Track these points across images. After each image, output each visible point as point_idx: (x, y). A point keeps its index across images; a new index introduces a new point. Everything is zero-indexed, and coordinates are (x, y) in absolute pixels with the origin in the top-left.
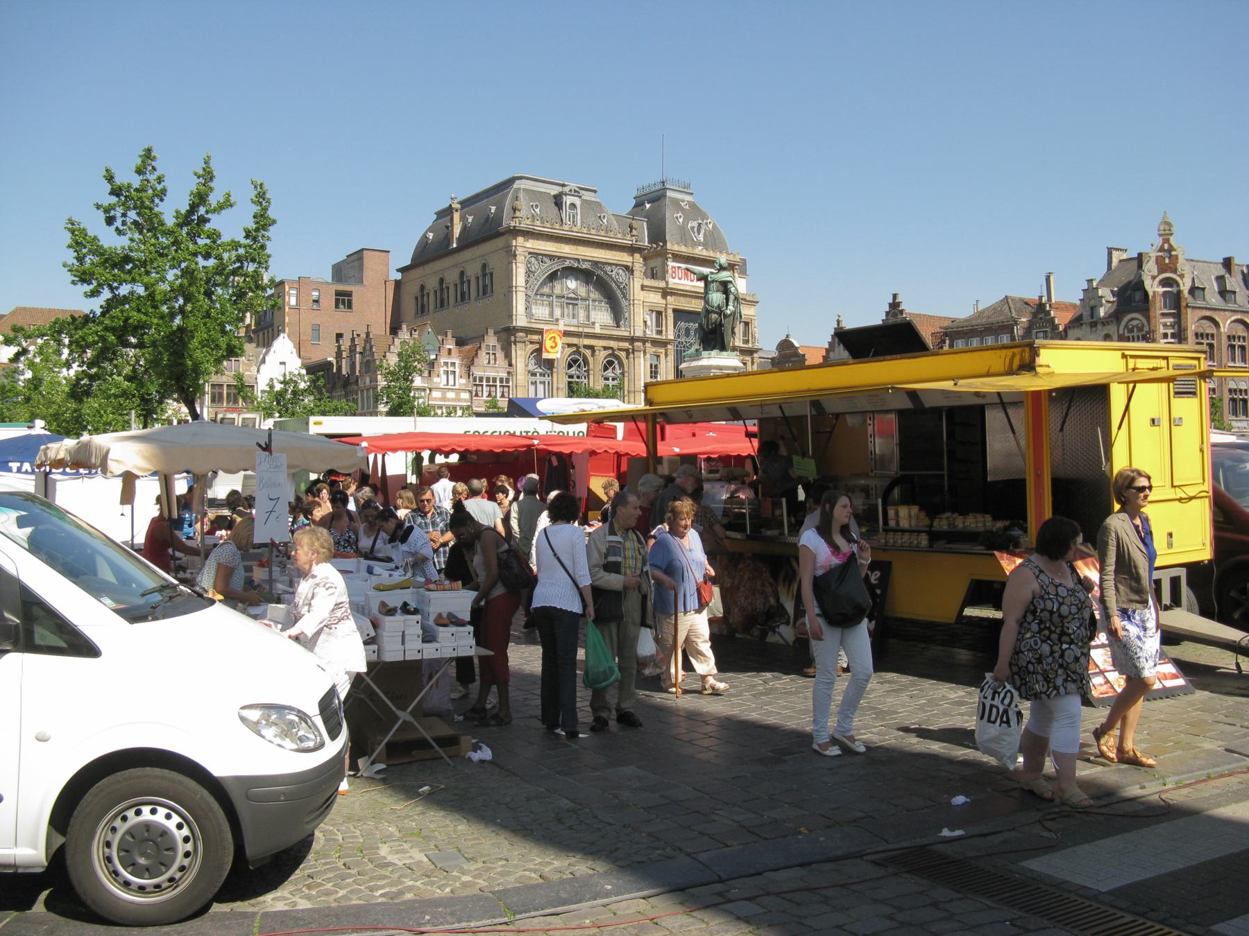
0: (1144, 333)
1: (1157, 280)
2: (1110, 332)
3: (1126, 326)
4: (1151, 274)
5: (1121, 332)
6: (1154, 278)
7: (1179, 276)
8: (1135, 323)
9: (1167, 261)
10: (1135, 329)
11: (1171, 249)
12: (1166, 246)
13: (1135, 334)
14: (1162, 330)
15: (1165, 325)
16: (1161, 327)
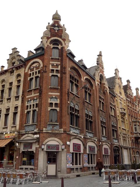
0: (40, 69)
1: (50, 40)
2: (20, 73)
3: (29, 68)
4: (47, 36)
5: (26, 71)
6: (48, 38)
7: (63, 39)
8: (34, 65)
9: (56, 31)
10: (35, 69)
11: (59, 26)
12: (56, 25)
13: (34, 71)
14: (51, 68)
15: (53, 65)
16: (51, 66)
